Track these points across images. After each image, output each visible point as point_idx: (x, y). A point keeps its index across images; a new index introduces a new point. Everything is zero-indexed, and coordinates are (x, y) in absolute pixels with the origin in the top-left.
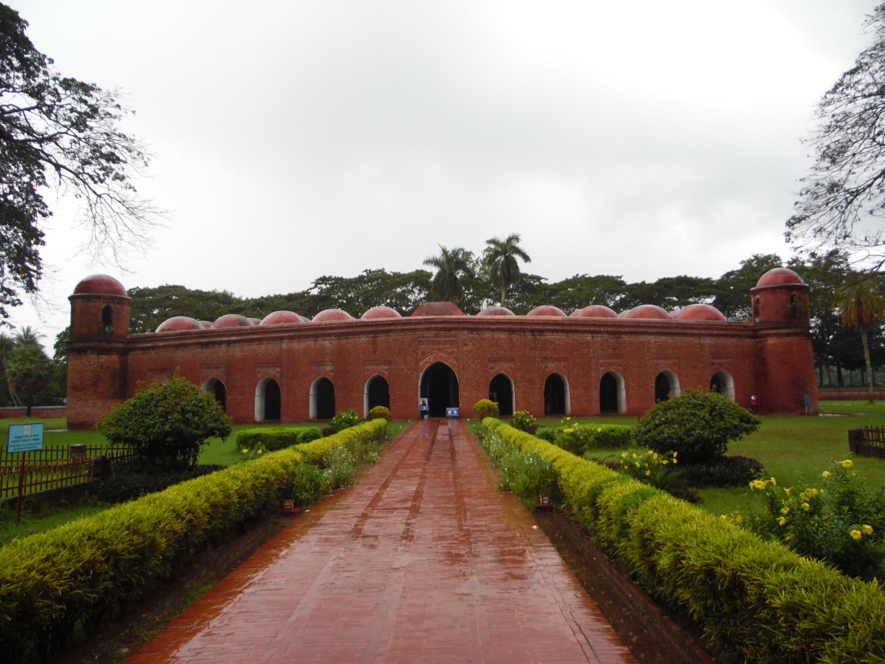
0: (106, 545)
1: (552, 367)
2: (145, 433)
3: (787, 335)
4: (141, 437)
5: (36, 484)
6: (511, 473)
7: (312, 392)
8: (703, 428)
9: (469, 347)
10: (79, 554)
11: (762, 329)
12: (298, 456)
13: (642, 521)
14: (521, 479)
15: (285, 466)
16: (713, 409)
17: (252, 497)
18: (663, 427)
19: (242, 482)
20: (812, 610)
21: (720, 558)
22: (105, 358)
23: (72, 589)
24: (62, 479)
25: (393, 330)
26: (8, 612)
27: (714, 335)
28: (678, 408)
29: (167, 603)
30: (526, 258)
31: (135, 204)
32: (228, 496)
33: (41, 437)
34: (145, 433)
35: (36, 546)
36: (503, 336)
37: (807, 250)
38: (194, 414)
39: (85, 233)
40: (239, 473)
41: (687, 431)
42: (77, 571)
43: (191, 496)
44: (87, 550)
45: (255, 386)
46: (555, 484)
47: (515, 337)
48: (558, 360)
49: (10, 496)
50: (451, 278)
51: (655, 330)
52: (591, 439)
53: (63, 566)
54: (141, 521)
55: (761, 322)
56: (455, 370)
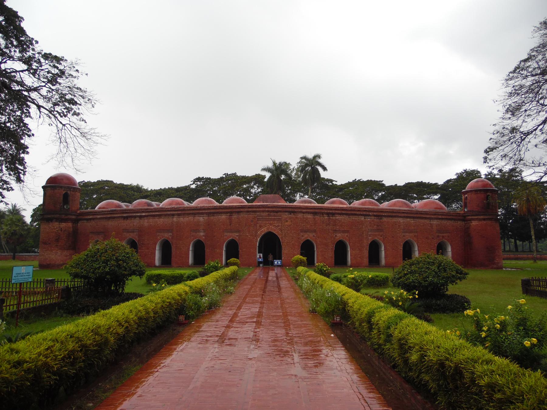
0: (81, 341)
1: (339, 236)
2: (93, 273)
3: (484, 219)
4: (91, 275)
5: (27, 302)
6: (317, 302)
7: (191, 249)
8: (434, 277)
9: (289, 223)
10: (66, 346)
11: (469, 216)
12: (187, 289)
13: (400, 333)
14: (323, 306)
15: (180, 295)
16: (440, 265)
17: (161, 314)
18: (409, 275)
19: (156, 304)
20: (503, 387)
21: (448, 356)
22: (63, 225)
23: (62, 367)
24: (42, 300)
25: (241, 212)
26: (27, 380)
27: (439, 219)
28: (419, 264)
29: (113, 377)
30: (325, 169)
31: (86, 131)
32: (148, 313)
33: (31, 274)
34: (93, 273)
35: (41, 340)
36: (310, 216)
37: (497, 168)
38: (124, 261)
39: (54, 148)
40: (153, 298)
41: (424, 278)
42: (64, 357)
43: (127, 312)
44: (70, 343)
45: (156, 244)
46: (344, 309)
47: (317, 217)
48: (344, 232)
49: (11, 310)
50: (278, 179)
51: (403, 215)
52: (365, 282)
53: (57, 353)
54: (100, 327)
55: (468, 211)
56: (280, 237)
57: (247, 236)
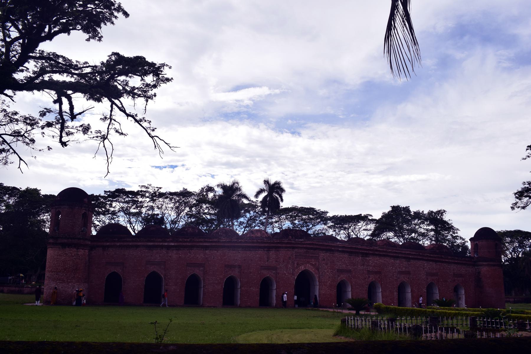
3: (494, 266)
25: (279, 247)
36: (346, 256)
57: (285, 274)
